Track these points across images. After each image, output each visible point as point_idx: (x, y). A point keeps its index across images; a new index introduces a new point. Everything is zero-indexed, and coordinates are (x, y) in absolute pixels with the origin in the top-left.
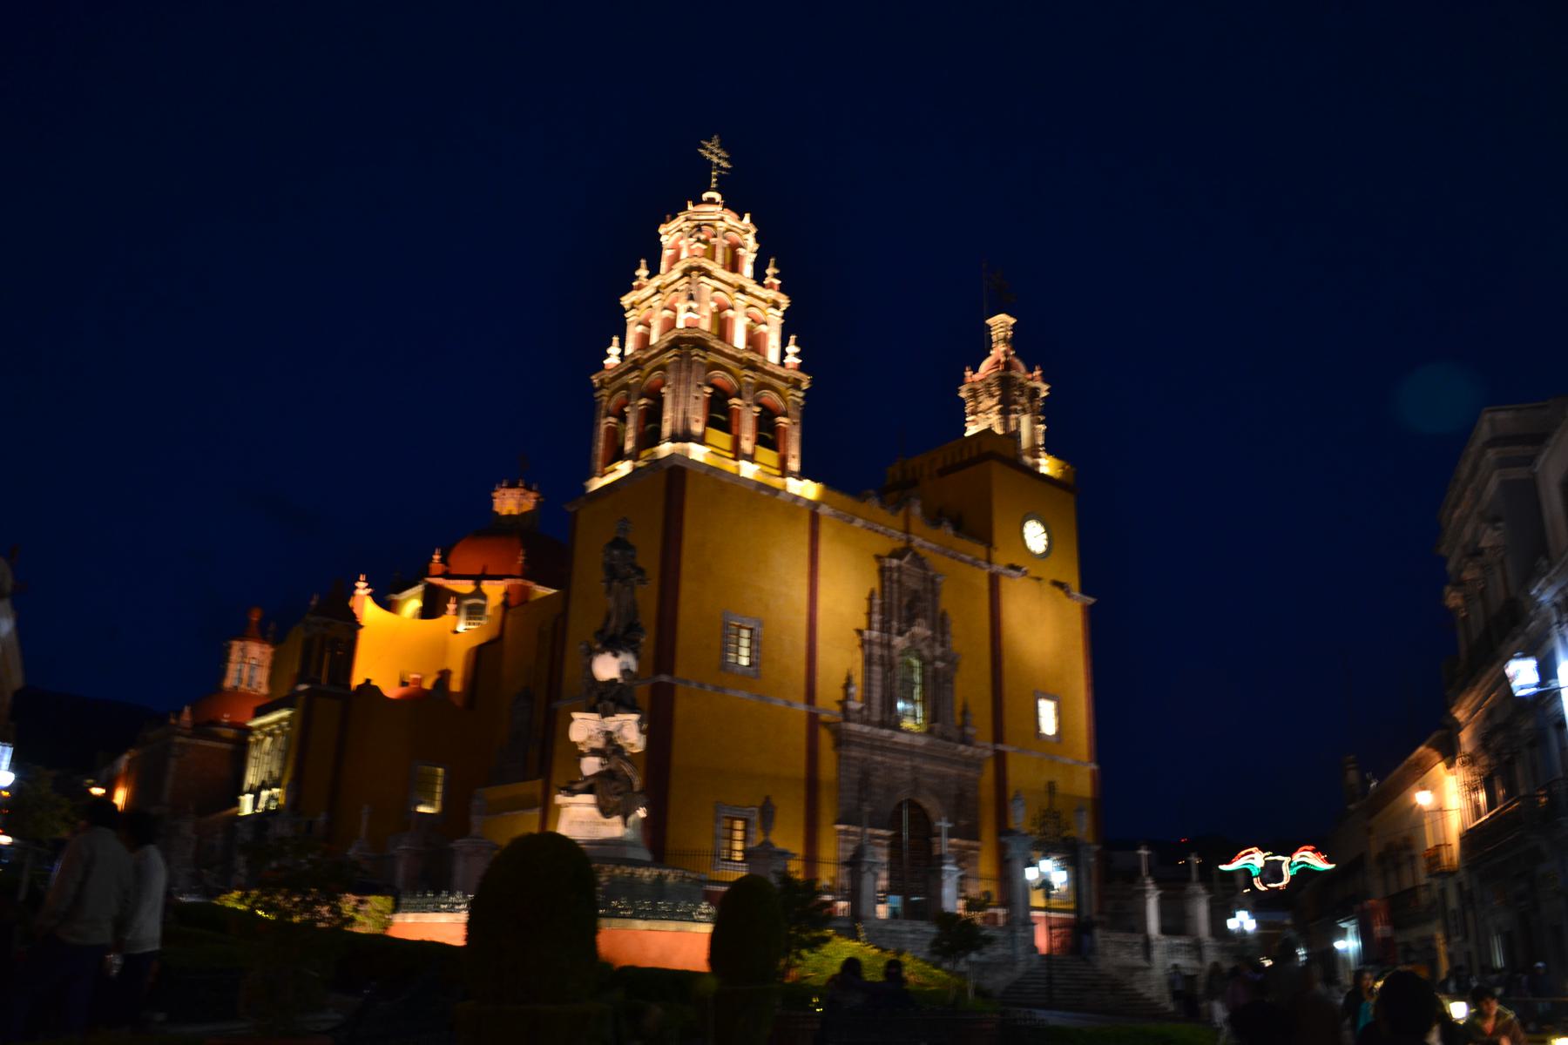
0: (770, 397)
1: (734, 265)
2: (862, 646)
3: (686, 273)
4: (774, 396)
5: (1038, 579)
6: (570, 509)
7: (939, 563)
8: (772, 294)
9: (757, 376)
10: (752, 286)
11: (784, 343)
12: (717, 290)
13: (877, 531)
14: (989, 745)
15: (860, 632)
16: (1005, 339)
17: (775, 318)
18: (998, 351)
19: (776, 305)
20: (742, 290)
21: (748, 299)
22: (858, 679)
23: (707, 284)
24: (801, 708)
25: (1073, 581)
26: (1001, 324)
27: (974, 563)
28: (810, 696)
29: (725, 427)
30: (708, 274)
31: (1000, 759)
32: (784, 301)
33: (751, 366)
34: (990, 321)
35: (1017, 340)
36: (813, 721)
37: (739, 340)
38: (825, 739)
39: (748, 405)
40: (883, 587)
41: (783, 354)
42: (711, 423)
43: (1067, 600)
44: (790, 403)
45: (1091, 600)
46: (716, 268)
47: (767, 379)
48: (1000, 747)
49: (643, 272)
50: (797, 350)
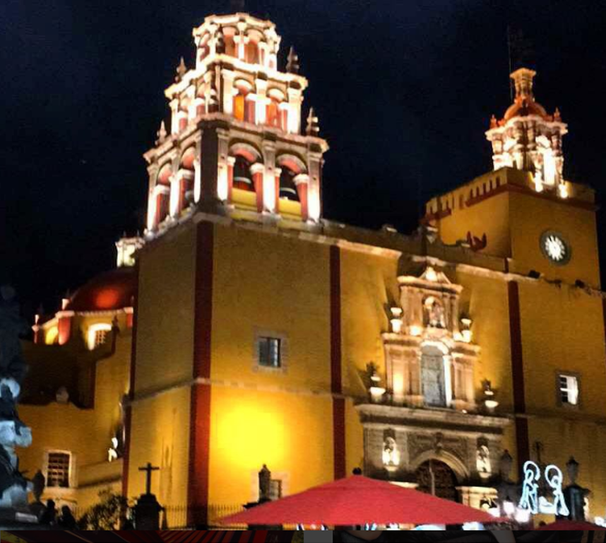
3: (211, 67)
4: (295, 159)
5: (558, 282)
8: (289, 77)
9: (279, 145)
12: (237, 79)
17: (296, 96)
19: (295, 85)
20: (262, 76)
23: (229, 75)
30: (230, 67)
32: (303, 82)
33: (271, 137)
34: (513, 75)
37: (260, 116)
39: (270, 169)
41: (304, 123)
44: (309, 164)
47: (287, 146)
50: (316, 120)
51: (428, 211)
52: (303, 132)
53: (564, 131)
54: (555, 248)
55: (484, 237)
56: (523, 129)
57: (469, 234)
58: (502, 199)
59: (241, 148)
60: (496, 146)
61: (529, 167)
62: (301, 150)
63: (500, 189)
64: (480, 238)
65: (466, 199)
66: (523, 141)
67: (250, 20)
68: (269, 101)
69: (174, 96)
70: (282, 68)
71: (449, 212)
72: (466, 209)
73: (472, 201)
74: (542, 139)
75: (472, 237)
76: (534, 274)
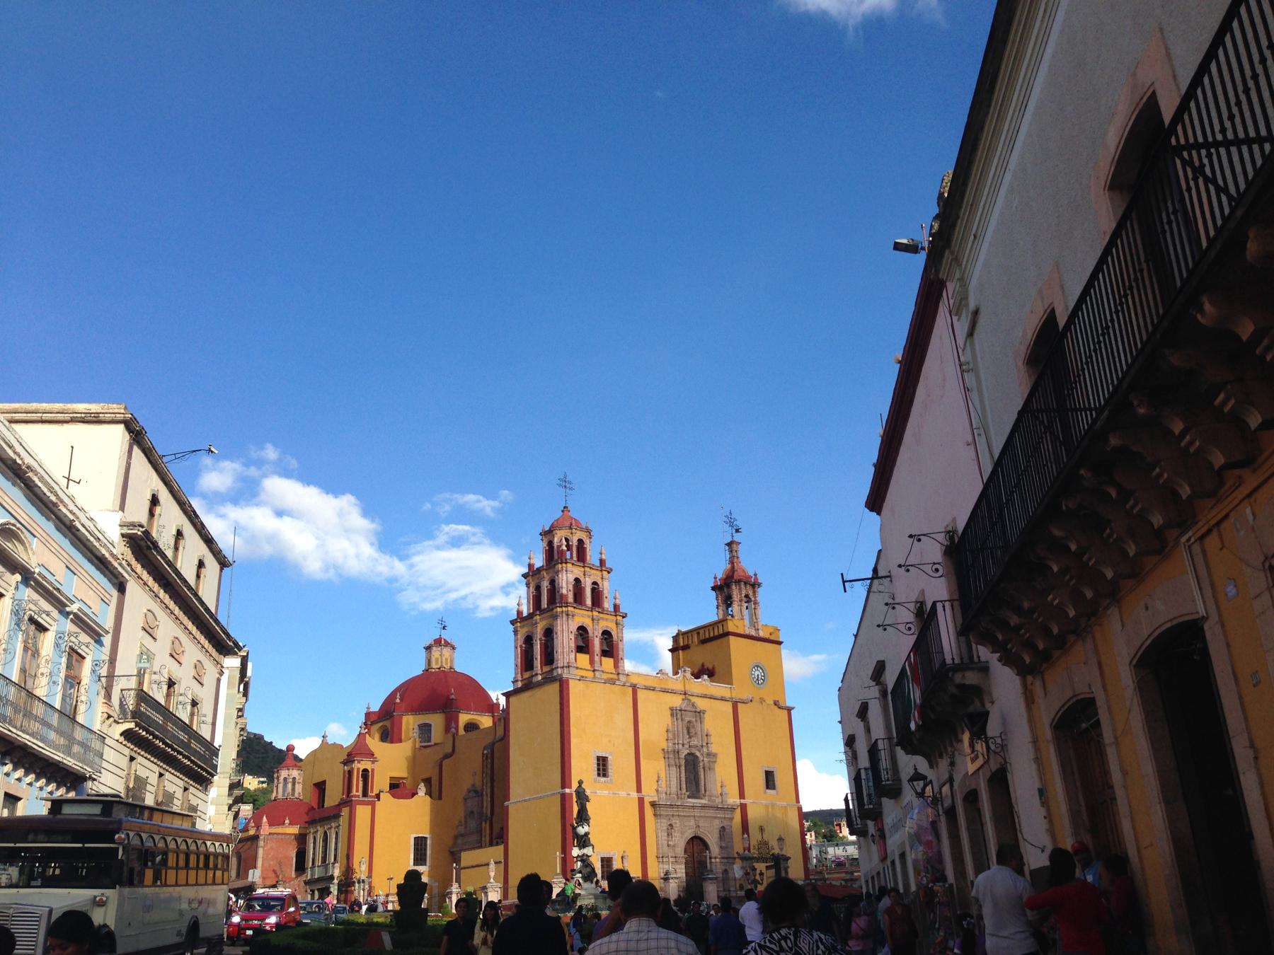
2: (664, 758)
7: (701, 704)
13: (668, 692)
14: (738, 801)
15: (663, 750)
22: (663, 775)
24: (635, 795)
27: (723, 699)
28: (639, 790)
31: (743, 807)
36: (641, 801)
38: (649, 811)
39: (597, 637)
40: (673, 722)
42: (580, 649)
43: (779, 710)
48: (743, 801)
55: (713, 668)
57: (703, 665)
64: (710, 667)
75: (705, 667)
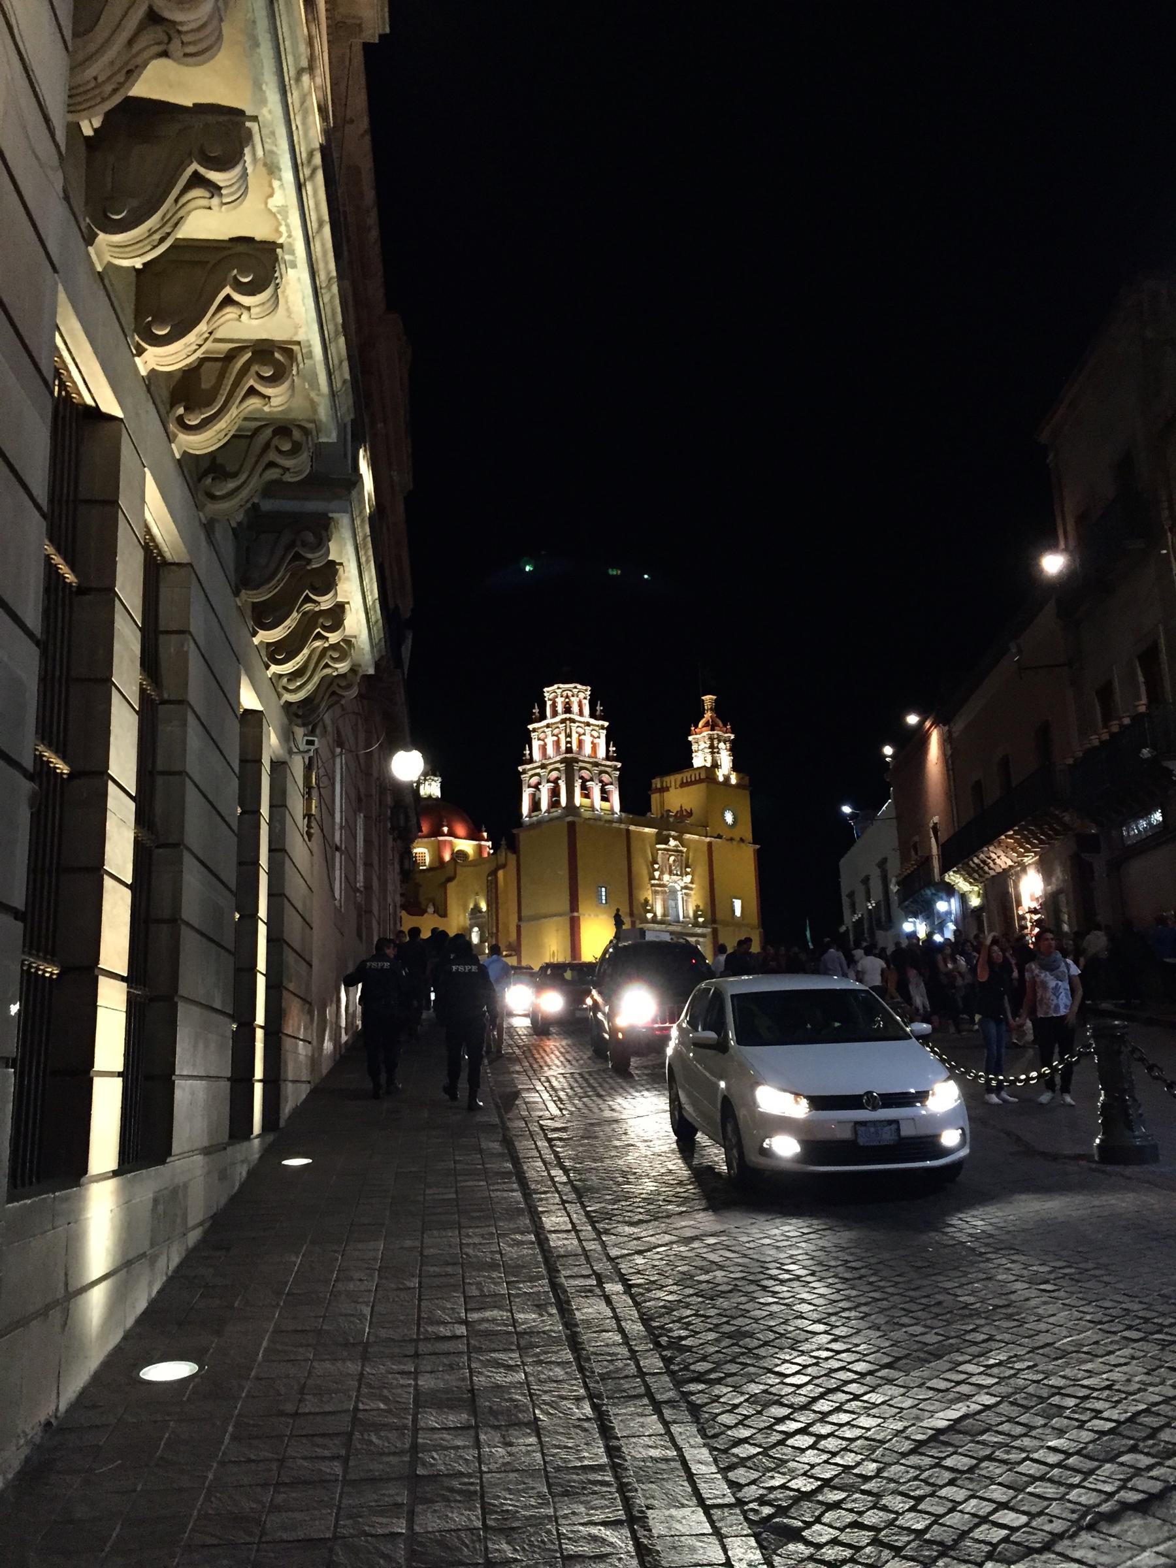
0: (605, 778)
1: (581, 714)
3: (563, 721)
5: (732, 839)
6: (515, 831)
8: (600, 723)
10: (592, 721)
11: (608, 746)
16: (711, 709)
18: (708, 715)
19: (602, 727)
20: (588, 724)
21: (592, 727)
25: (749, 836)
26: (708, 699)
29: (587, 796)
33: (596, 764)
35: (717, 708)
41: (608, 751)
45: (758, 847)
46: (578, 718)
47: (603, 768)
49: (536, 710)
51: (654, 786)
52: (608, 758)
53: (732, 737)
54: (729, 817)
56: (711, 739)
58: (703, 786)
59: (585, 774)
60: (694, 747)
61: (715, 765)
62: (608, 770)
63: (700, 781)
65: (678, 783)
66: (712, 747)
67: (579, 686)
68: (592, 739)
69: (534, 730)
70: (593, 715)
71: (667, 789)
72: (679, 790)
73: (683, 785)
74: (722, 745)
76: (719, 837)
